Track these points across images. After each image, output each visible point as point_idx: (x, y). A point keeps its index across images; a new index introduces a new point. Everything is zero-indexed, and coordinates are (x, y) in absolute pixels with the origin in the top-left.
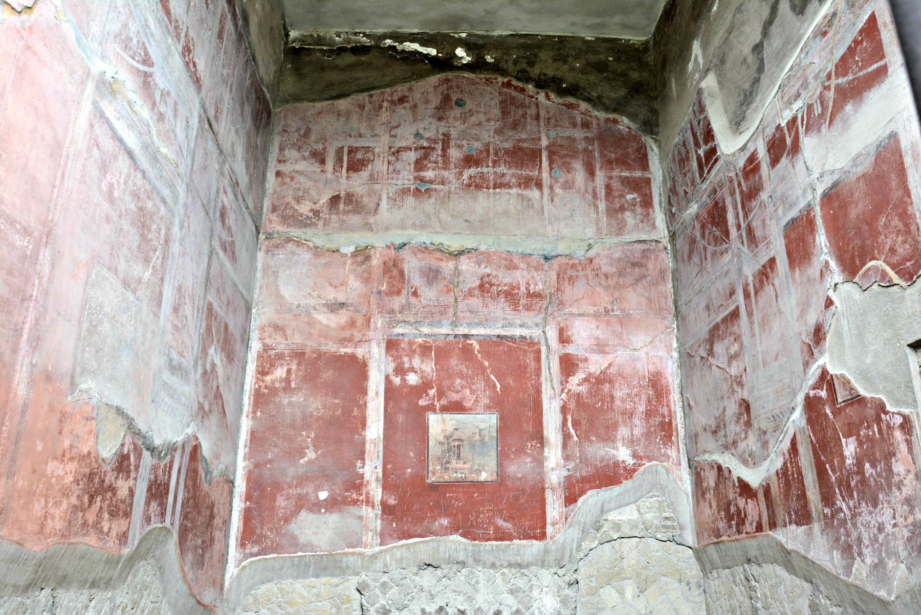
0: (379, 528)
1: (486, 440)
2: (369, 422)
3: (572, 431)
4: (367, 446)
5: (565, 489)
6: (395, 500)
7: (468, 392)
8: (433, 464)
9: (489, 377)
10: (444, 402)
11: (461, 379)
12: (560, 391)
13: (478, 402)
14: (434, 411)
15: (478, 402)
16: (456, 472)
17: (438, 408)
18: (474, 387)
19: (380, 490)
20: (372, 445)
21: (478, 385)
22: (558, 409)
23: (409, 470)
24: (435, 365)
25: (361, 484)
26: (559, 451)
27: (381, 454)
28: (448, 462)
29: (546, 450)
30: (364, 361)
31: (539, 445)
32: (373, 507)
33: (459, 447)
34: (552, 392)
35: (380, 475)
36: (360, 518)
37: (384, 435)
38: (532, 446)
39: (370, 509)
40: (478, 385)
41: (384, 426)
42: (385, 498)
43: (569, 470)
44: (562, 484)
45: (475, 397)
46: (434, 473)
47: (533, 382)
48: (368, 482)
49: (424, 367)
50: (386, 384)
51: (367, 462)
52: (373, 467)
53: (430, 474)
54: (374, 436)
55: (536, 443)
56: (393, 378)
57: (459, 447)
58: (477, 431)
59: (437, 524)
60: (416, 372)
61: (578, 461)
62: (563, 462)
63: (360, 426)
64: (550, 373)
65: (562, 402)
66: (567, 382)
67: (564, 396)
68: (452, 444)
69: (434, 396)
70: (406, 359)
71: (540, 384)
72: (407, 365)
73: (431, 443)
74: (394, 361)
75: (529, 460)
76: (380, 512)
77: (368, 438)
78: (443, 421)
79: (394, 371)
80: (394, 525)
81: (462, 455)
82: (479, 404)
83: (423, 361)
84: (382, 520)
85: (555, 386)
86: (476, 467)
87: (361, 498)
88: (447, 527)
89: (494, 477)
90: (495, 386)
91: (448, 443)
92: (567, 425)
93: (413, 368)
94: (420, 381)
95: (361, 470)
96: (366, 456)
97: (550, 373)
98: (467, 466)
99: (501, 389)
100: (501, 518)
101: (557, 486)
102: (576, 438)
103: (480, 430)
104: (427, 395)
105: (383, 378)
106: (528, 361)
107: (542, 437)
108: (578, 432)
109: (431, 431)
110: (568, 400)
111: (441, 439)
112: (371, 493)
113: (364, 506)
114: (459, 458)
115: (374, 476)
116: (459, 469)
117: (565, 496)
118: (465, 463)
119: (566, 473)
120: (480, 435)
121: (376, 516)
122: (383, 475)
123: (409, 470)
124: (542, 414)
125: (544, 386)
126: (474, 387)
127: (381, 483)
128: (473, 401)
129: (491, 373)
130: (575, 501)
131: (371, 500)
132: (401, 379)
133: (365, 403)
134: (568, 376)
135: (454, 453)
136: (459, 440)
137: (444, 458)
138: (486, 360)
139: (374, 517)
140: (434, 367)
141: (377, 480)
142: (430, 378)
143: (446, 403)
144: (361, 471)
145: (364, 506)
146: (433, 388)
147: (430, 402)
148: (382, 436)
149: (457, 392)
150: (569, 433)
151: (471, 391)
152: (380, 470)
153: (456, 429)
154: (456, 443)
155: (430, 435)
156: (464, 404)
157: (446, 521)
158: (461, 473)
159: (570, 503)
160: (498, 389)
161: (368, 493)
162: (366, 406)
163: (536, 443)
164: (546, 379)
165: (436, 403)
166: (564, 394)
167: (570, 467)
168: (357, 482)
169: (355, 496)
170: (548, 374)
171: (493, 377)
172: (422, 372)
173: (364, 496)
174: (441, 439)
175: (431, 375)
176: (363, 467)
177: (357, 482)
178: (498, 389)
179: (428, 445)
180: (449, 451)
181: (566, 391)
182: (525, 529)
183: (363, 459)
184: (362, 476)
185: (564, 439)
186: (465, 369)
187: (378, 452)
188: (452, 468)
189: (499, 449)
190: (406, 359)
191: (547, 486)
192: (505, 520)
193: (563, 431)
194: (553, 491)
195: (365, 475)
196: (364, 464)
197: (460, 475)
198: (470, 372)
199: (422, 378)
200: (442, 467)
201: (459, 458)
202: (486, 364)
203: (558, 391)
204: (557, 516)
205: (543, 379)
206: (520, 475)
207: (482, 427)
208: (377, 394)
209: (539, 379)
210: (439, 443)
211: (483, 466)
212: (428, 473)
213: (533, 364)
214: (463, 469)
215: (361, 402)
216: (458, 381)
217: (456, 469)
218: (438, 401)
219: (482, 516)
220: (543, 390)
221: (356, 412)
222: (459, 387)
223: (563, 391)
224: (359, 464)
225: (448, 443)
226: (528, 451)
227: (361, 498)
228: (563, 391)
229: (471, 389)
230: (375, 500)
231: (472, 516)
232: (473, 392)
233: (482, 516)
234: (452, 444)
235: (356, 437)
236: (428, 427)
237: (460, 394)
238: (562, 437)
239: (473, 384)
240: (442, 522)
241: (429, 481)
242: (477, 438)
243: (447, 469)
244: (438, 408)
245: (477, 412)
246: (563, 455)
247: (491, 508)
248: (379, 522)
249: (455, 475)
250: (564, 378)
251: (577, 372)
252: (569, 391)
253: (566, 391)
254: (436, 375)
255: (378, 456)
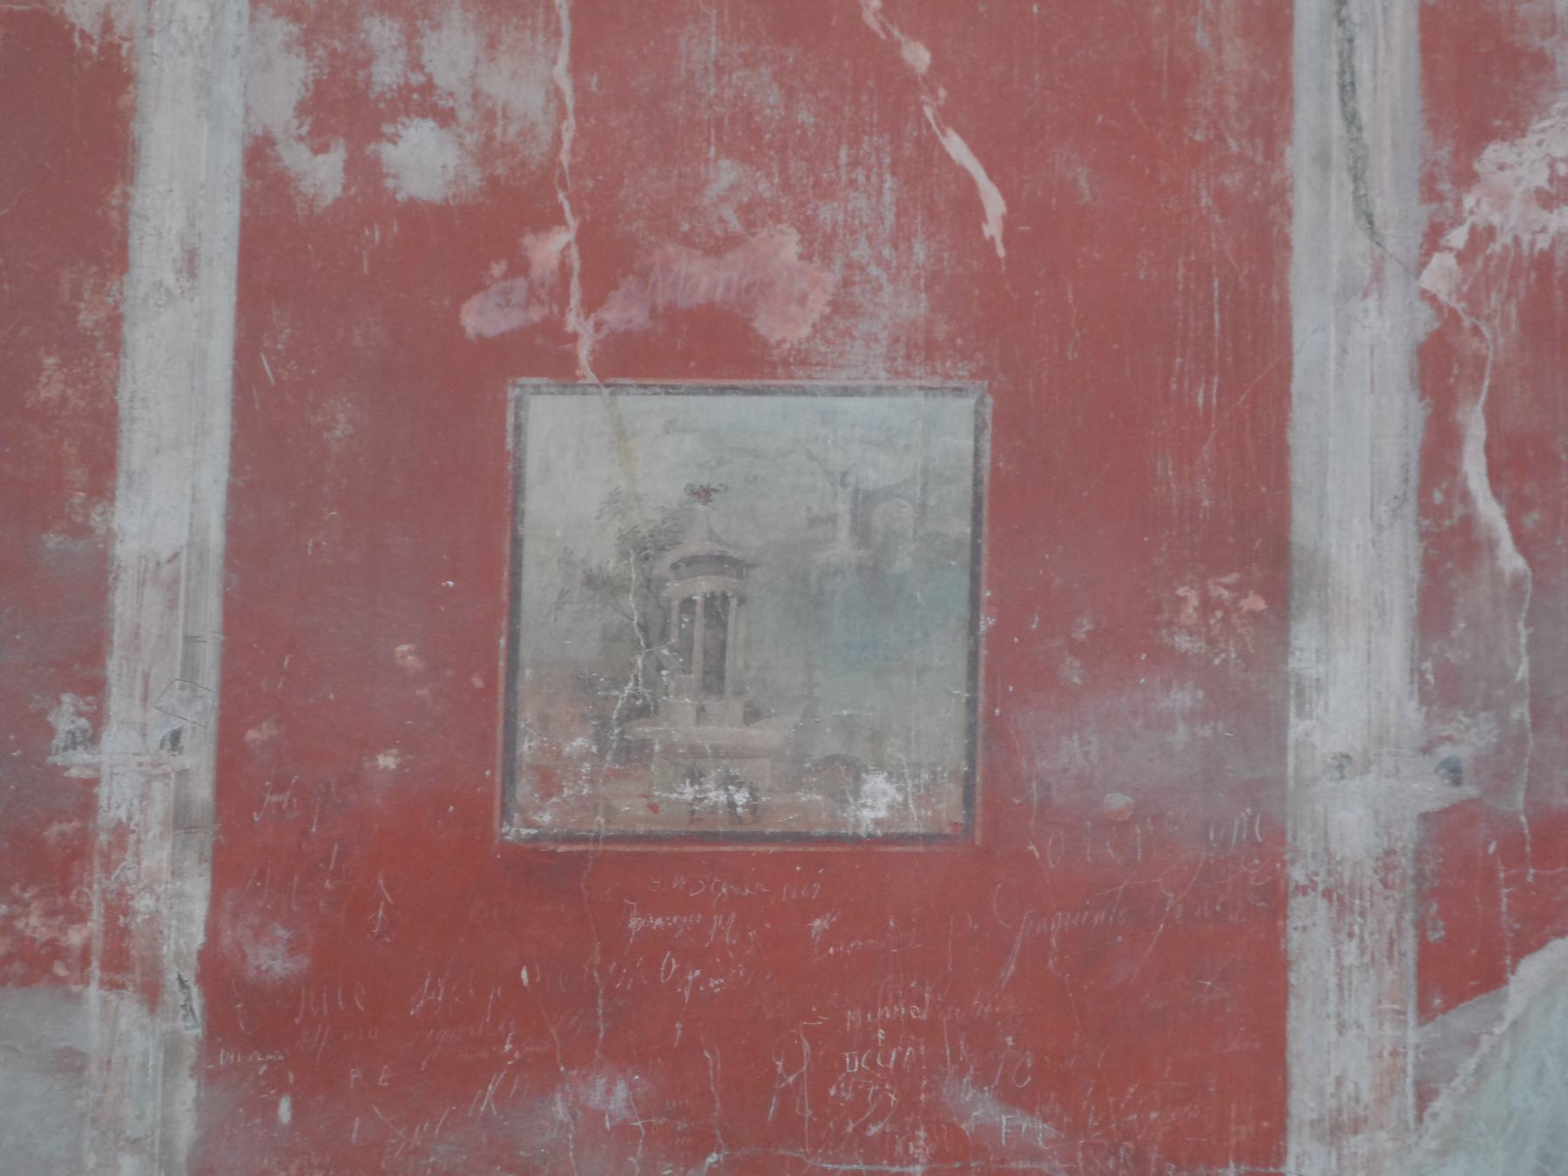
0: (186, 1131)
1: (902, 563)
2: (135, 448)
3: (1490, 512)
4: (122, 603)
5: (1422, 897)
6: (293, 950)
7: (789, 246)
8: (544, 720)
9: (930, 149)
10: (623, 313)
11: (745, 158)
12: (1415, 239)
13: (854, 310)
14: (562, 371)
15: (854, 310)
16: (695, 777)
17: (584, 352)
18: (827, 213)
19: (197, 890)
20: (154, 600)
21: (860, 202)
22: (1397, 362)
23: (387, 761)
24: (576, 69)
25: (78, 851)
26: (1395, 645)
27: (209, 655)
28: (641, 711)
29: (1304, 636)
30: (111, 50)
31: (1260, 604)
32: (151, 993)
33: (716, 608)
34: (1363, 243)
35: (203, 791)
36: (70, 1064)
37: (233, 529)
38: (1207, 606)
39: (129, 1009)
40: (860, 202)
41: (236, 469)
42: (226, 939)
43: (1454, 772)
44: (1406, 864)
45: (831, 278)
46: (548, 783)
47: (1233, 180)
48: (120, 832)
49: (498, 85)
50: (248, 200)
51: (116, 703)
52: (158, 734)
53: (524, 788)
54: (170, 535)
55: (1240, 589)
56: (295, 157)
57: (716, 608)
58: (843, 507)
59: (560, 1110)
60: (445, 118)
61: (1520, 712)
62: (1414, 714)
63: (78, 474)
64: (1351, 119)
65: (1425, 313)
66: (1466, 178)
67: (1441, 274)
68: (674, 589)
69: (564, 270)
70: (381, 32)
71: (1280, 196)
72: (387, 74)
73: (538, 583)
74: (307, 42)
75: (1182, 698)
76: (192, 1030)
77: (126, 551)
78: (621, 436)
79: (302, 109)
80: (285, 1111)
81: (735, 660)
82: (863, 327)
83: (492, 44)
84: (210, 1076)
85: (1384, 206)
86: (829, 744)
87: (75, 937)
88: (624, 1132)
89: (949, 807)
90: (971, 207)
91: (650, 586)
92: (1454, 471)
93: (429, 87)
94: (474, 178)
95: (80, 756)
96: (114, 667)
97: (1351, 119)
98: (770, 734)
99: (1009, 223)
100: (982, 1080)
101: (1370, 879)
102: (1511, 560)
103: (864, 500)
104: (519, 267)
105: (232, 155)
106: (1201, 37)
107: (1278, 552)
108: (1532, 519)
109: (538, 504)
110: (1474, 300)
111: (603, 554)
112: (144, 903)
113: (93, 992)
114: (714, 679)
115: (162, 798)
116: (718, 753)
117: (1423, 943)
118: (753, 715)
119: (1432, 792)
120: (861, 531)
121: (172, 1051)
122: (224, 789)
123: (387, 761)
124: (1282, 398)
125: (1304, 203)
126: (827, 213)
127: (205, 839)
128: (818, 304)
129: (948, 117)
130: (1492, 978)
131: (136, 947)
132: (350, 167)
133: (115, 321)
134: (1475, 135)
135: (686, 649)
136: (719, 562)
137: (617, 683)
138: (914, 33)
139: (156, 1059)
140: (566, 85)
141: (181, 820)
142: (536, 152)
143: (638, 317)
144: (77, 762)
145: (93, 992)
146: (559, 220)
147: (536, 314)
148: (216, 537)
149: (719, 246)
150: (1468, 522)
151: (807, 241)
152: (199, 760)
153: (704, 494)
154: (702, 586)
155: (527, 531)
156: (764, 324)
157: (621, 1091)
158: (728, 781)
159: (1457, 996)
160: (992, 228)
161: (118, 908)
162: (115, 343)
163: (1240, 589)
164: (1323, 160)
165: (573, 322)
166: (1443, 262)
167: (1463, 753)
168: (53, 832)
169: (34, 924)
170: (1337, 123)
171: (956, 147)
172: (489, 116)
173: (95, 923)
174: (603, 554)
175: (545, 134)
176: (93, 739)
177: (53, 832)
178: (992, 228)
179: (515, 593)
180: (653, 632)
181: (1458, 237)
182: (1139, 1157)
183: (94, 688)
184: (84, 796)
185: (1430, 566)
186: (774, 96)
187: (190, 640)
188: (669, 750)
189: (986, 623)
190: (381, 32)
191: (1297, 874)
192: (1010, 1097)
193: (1426, 508)
194: (1343, 908)
195: (103, 792)
196: (98, 719)
197: (717, 796)
198: (805, 116)
199: (486, 153)
200: (600, 738)
201: (714, 679)
202: (918, 56)
203: (1401, 239)
204: (1362, 1080)
205: (1299, 156)
206: (1117, 801)
207: (872, 478)
208: (190, 263)
209: (1273, 153)
210: (590, 581)
211: (877, 737)
212: (510, 775)
213: (1236, 56)
214: (739, 753)
215: (86, 319)
216: (725, 174)
217: (695, 751)
218: (592, 304)
219: (856, 1063)
220: (1301, 231)
221: (51, 383)
222: (729, 213)
223: (1433, 238)
224: (66, 717)
225: (650, 586)
226: (1183, 642)
227: (75, 937)
228: (1433, 238)
229: (807, 227)
230: (167, 950)
231: (793, 1064)
232: (817, 244)
233: (856, 1063)
234: (674, 589)
235: (53, 541)
236: (518, 478)
237: (736, 257)
238: (1415, 548)
239: (825, 191)
240: (596, 1098)
241: (513, 832)
242: (842, 548)
243: (634, 754)
244: (584, 352)
245: (841, 379)
246: (1416, 671)
247: (916, 1013)
248: (188, 1089)
249: (689, 792)
250: (1444, 154)
251: (1543, 112)
252: (1481, 237)
253: (1458, 237)
254: (581, 134)
255: (190, 672)
